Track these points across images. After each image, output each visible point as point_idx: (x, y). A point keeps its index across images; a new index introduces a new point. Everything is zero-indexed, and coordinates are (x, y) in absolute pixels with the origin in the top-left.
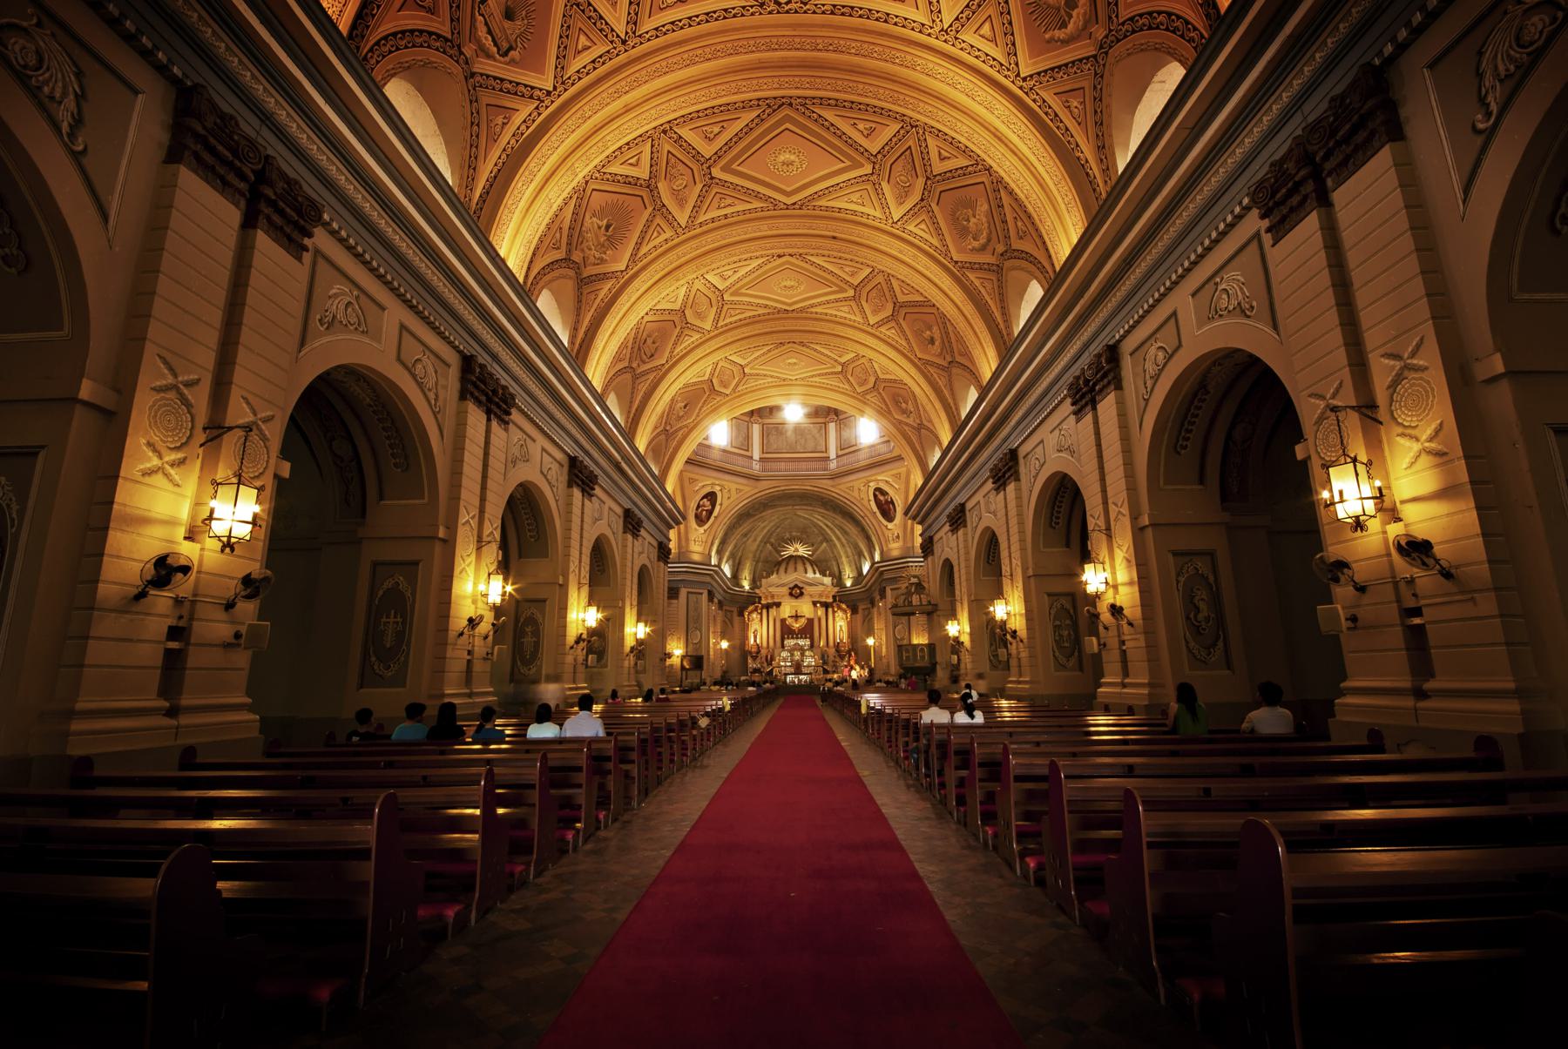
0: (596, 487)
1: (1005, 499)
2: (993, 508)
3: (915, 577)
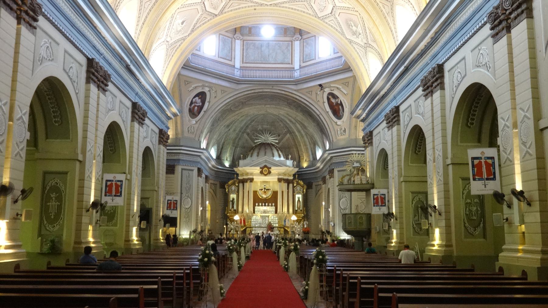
0: (110, 84)
1: (432, 103)
2: (421, 110)
3: (357, 162)
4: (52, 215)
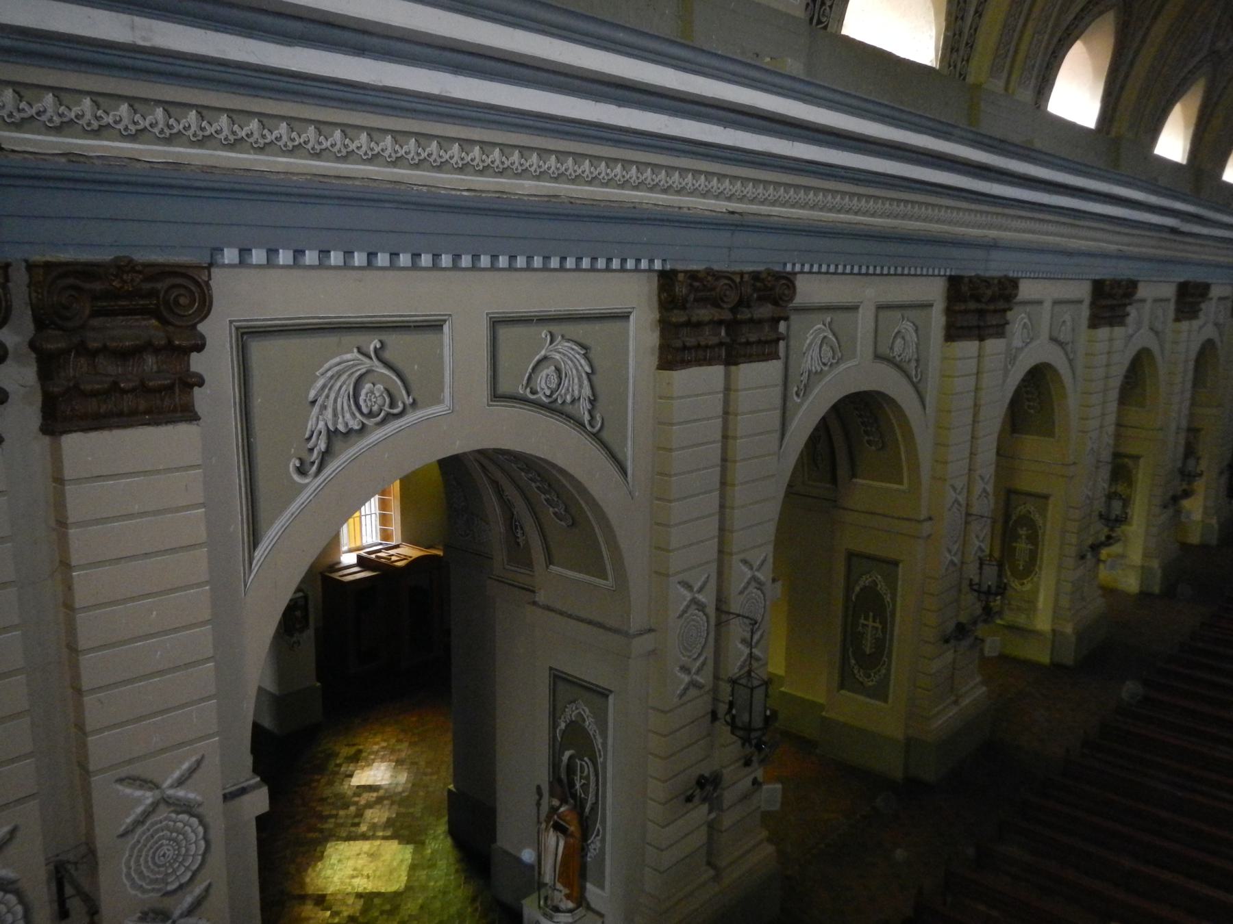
4: (1019, 565)
